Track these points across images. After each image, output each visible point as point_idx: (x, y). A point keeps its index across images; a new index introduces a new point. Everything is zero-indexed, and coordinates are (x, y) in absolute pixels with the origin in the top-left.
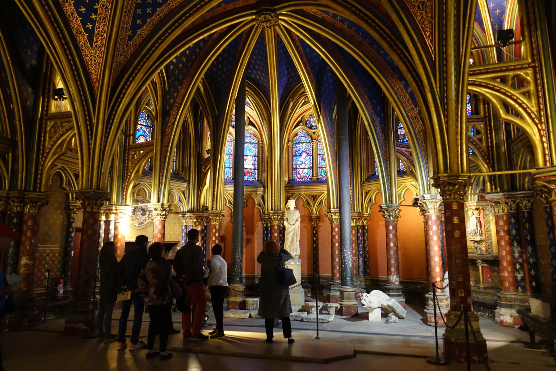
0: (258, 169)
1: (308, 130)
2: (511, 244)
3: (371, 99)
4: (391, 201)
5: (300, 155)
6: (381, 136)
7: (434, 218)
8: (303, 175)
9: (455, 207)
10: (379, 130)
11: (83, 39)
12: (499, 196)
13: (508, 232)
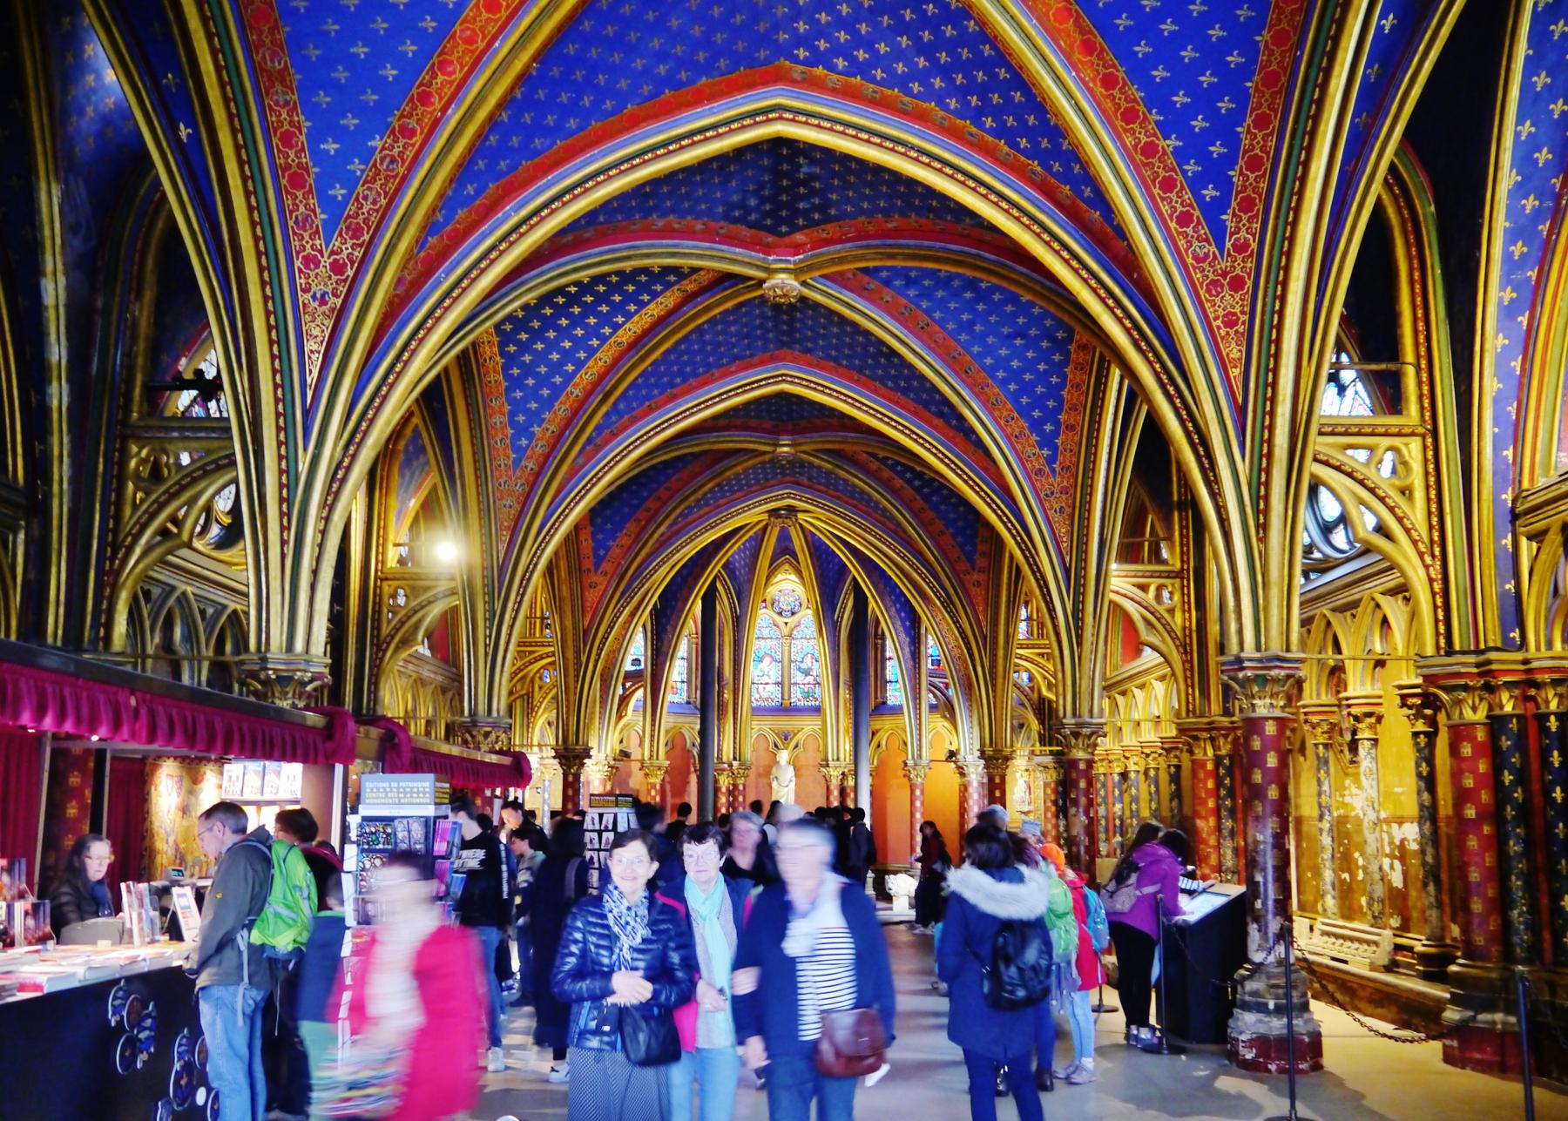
0: (689, 682)
1: (777, 617)
2: (1057, 817)
3: (898, 612)
4: (920, 756)
5: (761, 660)
6: (910, 663)
7: (975, 784)
8: (764, 695)
9: (997, 780)
10: (908, 655)
11: (588, 563)
12: (1048, 760)
13: (1055, 803)
